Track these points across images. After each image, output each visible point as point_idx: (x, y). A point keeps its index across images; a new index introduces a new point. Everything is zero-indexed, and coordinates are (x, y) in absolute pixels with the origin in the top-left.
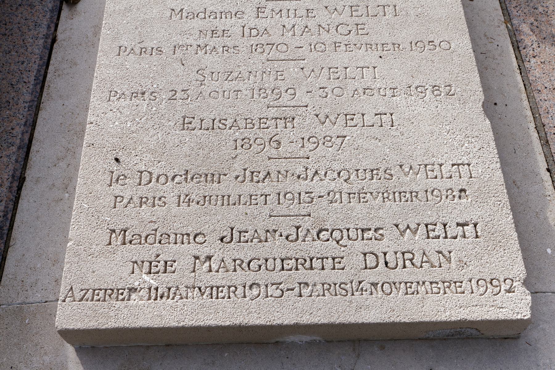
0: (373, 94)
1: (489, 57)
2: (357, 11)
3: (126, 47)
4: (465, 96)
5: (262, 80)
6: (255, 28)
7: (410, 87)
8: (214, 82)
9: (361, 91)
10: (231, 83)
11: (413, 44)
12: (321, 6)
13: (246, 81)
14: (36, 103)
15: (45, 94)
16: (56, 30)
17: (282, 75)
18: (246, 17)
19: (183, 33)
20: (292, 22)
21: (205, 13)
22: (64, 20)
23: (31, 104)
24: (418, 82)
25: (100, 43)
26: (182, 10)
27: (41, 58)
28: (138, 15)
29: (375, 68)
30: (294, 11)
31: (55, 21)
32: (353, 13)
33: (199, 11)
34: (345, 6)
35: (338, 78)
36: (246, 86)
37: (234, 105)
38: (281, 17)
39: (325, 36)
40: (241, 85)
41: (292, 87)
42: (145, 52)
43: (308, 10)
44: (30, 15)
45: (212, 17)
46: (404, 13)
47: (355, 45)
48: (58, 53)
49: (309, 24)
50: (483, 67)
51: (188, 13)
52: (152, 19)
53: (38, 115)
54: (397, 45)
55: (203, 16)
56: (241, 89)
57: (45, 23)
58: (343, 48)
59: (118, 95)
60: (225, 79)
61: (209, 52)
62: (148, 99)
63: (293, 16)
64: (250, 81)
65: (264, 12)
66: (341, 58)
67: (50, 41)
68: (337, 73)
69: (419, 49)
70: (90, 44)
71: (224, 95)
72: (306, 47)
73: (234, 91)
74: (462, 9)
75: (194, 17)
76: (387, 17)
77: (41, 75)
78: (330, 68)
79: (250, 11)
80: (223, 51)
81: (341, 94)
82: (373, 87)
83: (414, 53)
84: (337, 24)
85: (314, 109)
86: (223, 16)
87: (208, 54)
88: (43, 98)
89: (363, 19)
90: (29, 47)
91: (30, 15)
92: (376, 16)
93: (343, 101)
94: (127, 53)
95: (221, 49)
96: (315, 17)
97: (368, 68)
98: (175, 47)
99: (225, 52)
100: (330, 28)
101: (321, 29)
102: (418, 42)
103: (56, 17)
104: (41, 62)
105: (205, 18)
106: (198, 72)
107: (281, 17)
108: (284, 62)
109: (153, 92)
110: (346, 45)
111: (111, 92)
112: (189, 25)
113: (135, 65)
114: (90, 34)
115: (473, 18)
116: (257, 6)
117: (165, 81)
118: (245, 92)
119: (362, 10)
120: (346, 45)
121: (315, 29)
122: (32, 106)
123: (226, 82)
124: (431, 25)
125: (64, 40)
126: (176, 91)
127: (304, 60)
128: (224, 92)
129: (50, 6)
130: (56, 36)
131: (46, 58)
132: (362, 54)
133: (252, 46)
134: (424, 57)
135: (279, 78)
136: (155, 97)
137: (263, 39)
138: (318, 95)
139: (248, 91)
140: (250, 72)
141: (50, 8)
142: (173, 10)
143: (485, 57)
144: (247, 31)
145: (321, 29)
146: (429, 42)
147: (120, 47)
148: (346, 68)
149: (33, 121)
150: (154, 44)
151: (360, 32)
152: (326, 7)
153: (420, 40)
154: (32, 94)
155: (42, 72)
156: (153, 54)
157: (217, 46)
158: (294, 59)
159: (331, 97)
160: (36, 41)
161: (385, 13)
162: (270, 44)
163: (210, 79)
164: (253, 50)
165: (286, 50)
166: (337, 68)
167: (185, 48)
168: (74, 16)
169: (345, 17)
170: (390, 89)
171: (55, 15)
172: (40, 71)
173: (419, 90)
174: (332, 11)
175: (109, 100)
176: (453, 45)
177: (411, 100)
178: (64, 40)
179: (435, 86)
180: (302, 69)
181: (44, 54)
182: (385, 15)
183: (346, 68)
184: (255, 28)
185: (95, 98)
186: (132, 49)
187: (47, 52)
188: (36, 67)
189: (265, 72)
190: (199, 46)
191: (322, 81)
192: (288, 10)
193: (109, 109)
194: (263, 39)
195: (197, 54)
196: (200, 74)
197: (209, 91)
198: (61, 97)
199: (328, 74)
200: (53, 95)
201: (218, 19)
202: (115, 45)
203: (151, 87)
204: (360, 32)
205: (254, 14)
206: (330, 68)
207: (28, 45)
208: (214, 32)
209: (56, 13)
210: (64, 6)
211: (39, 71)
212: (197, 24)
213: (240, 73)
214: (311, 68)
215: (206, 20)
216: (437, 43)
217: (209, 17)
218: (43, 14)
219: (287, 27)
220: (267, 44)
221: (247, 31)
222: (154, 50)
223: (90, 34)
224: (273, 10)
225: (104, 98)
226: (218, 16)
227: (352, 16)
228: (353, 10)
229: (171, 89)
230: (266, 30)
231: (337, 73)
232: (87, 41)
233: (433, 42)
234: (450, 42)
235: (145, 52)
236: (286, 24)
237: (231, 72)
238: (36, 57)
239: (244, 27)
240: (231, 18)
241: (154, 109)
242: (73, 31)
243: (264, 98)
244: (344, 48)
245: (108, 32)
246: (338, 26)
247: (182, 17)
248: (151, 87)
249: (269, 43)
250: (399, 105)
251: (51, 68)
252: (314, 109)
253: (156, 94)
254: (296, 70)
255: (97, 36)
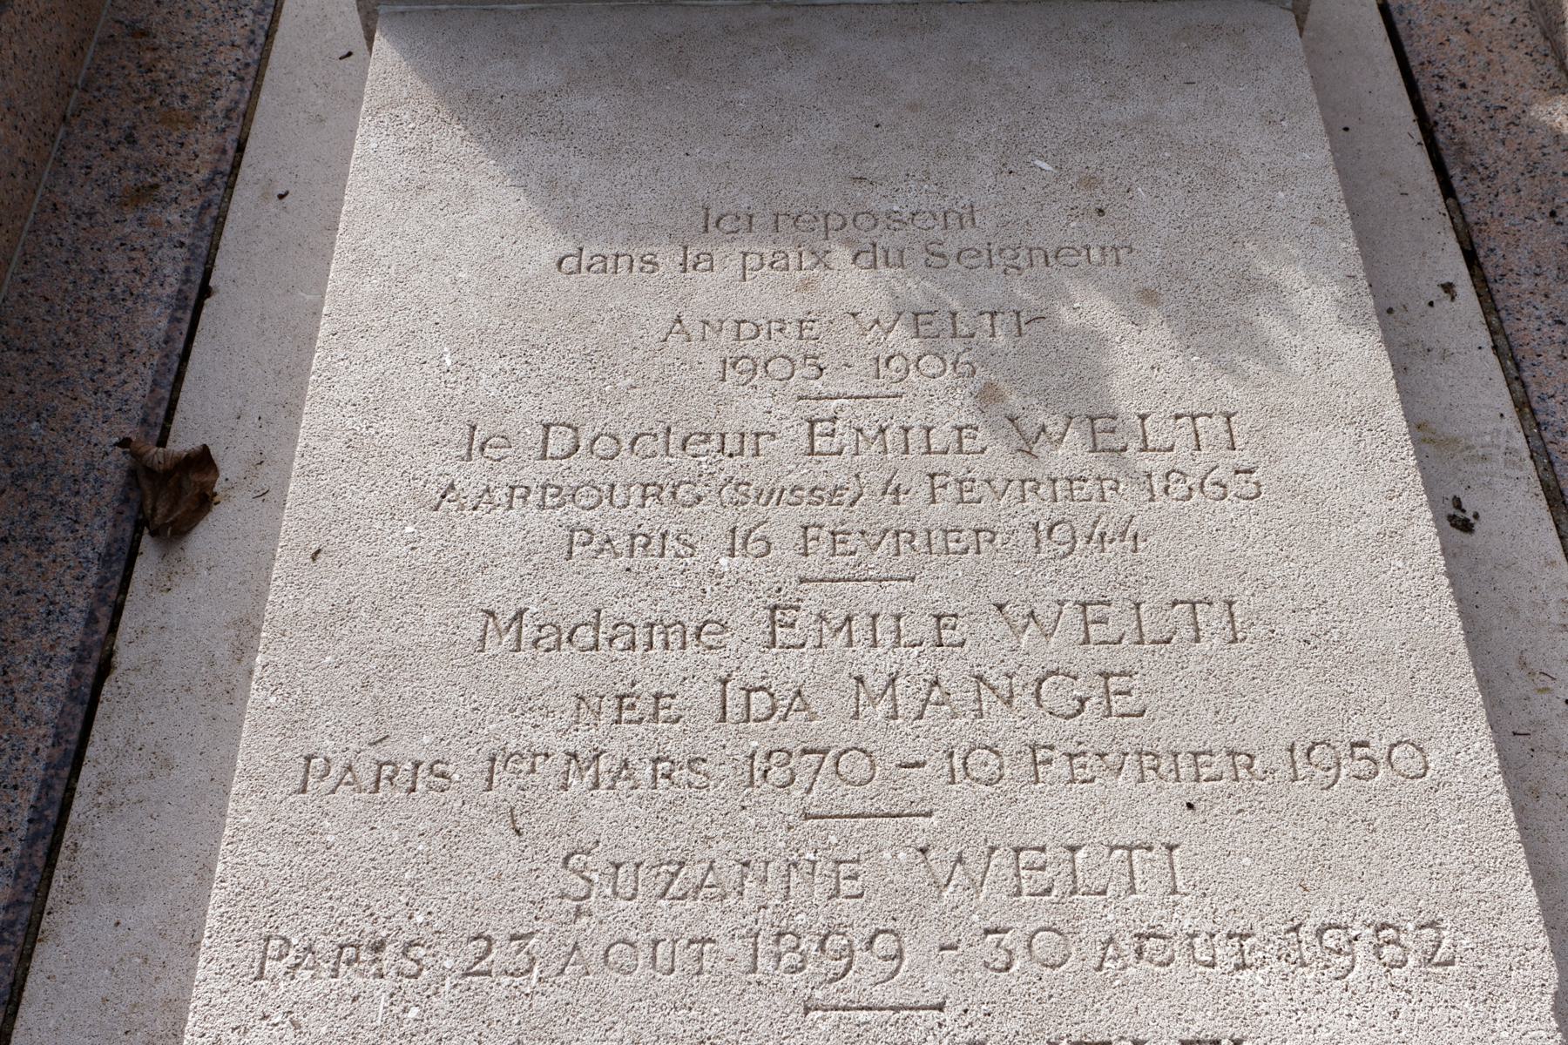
0: (1171, 959)
1: (1542, 748)
2: (1102, 621)
3: (327, 760)
4: (1492, 970)
5: (786, 898)
6: (762, 688)
7: (1295, 929)
8: (623, 904)
9: (1127, 945)
10: (678, 907)
11: (1298, 753)
12: (985, 601)
13: (731, 901)
14: (27, 912)
15: (59, 876)
16: (113, 628)
17: (855, 877)
18: (732, 643)
19: (523, 705)
20: (888, 665)
21: (596, 629)
22: (142, 594)
23: (11, 916)
24: (1324, 909)
25: (242, 744)
26: (520, 614)
27: (58, 737)
28: (374, 635)
29: (1171, 848)
30: (891, 622)
31: (113, 594)
32: (1092, 628)
33: (578, 619)
34: (1061, 603)
35: (1048, 891)
36: (730, 921)
37: (688, 1001)
38: (850, 644)
39: (998, 721)
40: (716, 921)
41: (890, 925)
42: (390, 779)
43: (939, 618)
44: (34, 575)
45: (619, 644)
46: (1260, 629)
47: (1102, 756)
48: (115, 717)
49: (944, 673)
50: (1525, 786)
51: (541, 627)
52: (419, 651)
53: (30, 957)
54: (1243, 758)
55: (590, 640)
56: (714, 934)
57: (81, 604)
58: (1060, 768)
59: (292, 952)
60: (659, 890)
61: (606, 780)
62: (393, 972)
63: (889, 639)
64: (745, 902)
65: (792, 625)
66: (1053, 809)
67: (90, 669)
68: (1042, 868)
69: (1319, 773)
70: (219, 687)
71: (654, 958)
72: (936, 762)
73: (691, 942)
74: (1454, 616)
75: (559, 641)
76: (1204, 646)
77: (51, 803)
78: (1018, 850)
79: (747, 623)
80: (655, 778)
81: (1058, 959)
82: (1168, 929)
83: (1304, 791)
84: (1038, 672)
85: (968, 1019)
86: (658, 640)
87: (602, 791)
88: (53, 893)
89: (1126, 656)
90: (20, 696)
91: (34, 575)
92: (1168, 641)
93: (1067, 986)
94: (329, 782)
95: (649, 769)
96: (962, 644)
97: (1150, 849)
98: (493, 760)
99: (662, 782)
100: (1017, 690)
101: (985, 691)
102: (1315, 744)
103: (118, 579)
104: (57, 754)
105: (596, 646)
106: (566, 860)
107: (850, 644)
108: (862, 821)
109: (411, 944)
110: (1071, 756)
111: (268, 939)
112: (542, 673)
113: (356, 833)
114: (222, 652)
115: (1479, 600)
116: (771, 601)
117: (453, 898)
118: (727, 948)
119: (1119, 621)
120: (1071, 756)
121: (963, 693)
122: (12, 924)
123: (663, 903)
124: (1357, 678)
125: (137, 669)
126: (489, 939)
127: (929, 814)
128: (656, 943)
129: (101, 538)
130: (111, 654)
131: (74, 737)
132: (1125, 794)
133: (752, 757)
134: (1338, 807)
135: (846, 886)
136: (418, 962)
137: (790, 732)
138: (980, 962)
139: (738, 942)
140: (746, 864)
141: (101, 549)
142: (491, 614)
143: (1527, 748)
144: (735, 697)
145: (985, 691)
146: (1354, 745)
147: (309, 759)
148: (1073, 849)
149: (13, 984)
150: (422, 747)
151: (1118, 703)
152: (1000, 607)
153: (1320, 738)
154: (17, 877)
155: (58, 793)
156: (419, 786)
157: (633, 759)
158: (896, 811)
159: (1023, 971)
160: (47, 672)
161: (1197, 630)
162: (813, 751)
163: (609, 891)
164: (757, 774)
165: (867, 776)
166: (1043, 849)
167: (525, 766)
168: (176, 579)
169: (1061, 647)
170: (1230, 936)
171: (116, 573)
172: (50, 787)
173: (1330, 940)
174: (1021, 622)
175: (260, 977)
176: (1434, 758)
177: (1303, 984)
178: (137, 669)
179: (1384, 926)
180: (924, 851)
181: (69, 720)
182: (1197, 640)
183: (1073, 849)
184: (762, 688)
185: (214, 966)
186: (350, 768)
187: (80, 711)
188: (38, 770)
189: (795, 865)
190: (575, 756)
191: (992, 901)
192: (875, 617)
193: (259, 1013)
194: (790, 732)
195: (565, 787)
196: (574, 871)
197: (604, 941)
198: (111, 890)
199: (1011, 871)
200: (87, 883)
201: (639, 652)
202: (292, 754)
203: (406, 925)
204: (1118, 703)
205: (759, 634)
206: (1018, 850)
207: (19, 687)
208: (627, 701)
209: (118, 567)
210: (146, 541)
211: (46, 785)
212: (570, 667)
213: (711, 868)
214: (954, 850)
215: (599, 656)
216: (1378, 749)
217: (611, 641)
218: (75, 572)
219: (869, 682)
220: (805, 752)
221: (735, 697)
222: (422, 772)
223: (222, 652)
224: (821, 617)
225: (242, 968)
226: (641, 639)
227: (1087, 641)
228: (1090, 618)
229: (473, 933)
230: (799, 693)
231: (1042, 868)
232: (210, 679)
233: (1364, 744)
234: (1425, 745)
235: (390, 779)
236: (866, 672)
237: (682, 864)
238: (41, 732)
239: (725, 683)
240: (684, 646)
241: (414, 1012)
242: (167, 635)
243: (794, 970)
244: (1066, 771)
245: (273, 700)
246: (1040, 681)
247: (519, 640)
248: (406, 925)
249: (809, 746)
250: (1263, 1006)
251: (86, 772)
252: (968, 1019)
253: (422, 951)
254: (901, 855)
255: (245, 661)
